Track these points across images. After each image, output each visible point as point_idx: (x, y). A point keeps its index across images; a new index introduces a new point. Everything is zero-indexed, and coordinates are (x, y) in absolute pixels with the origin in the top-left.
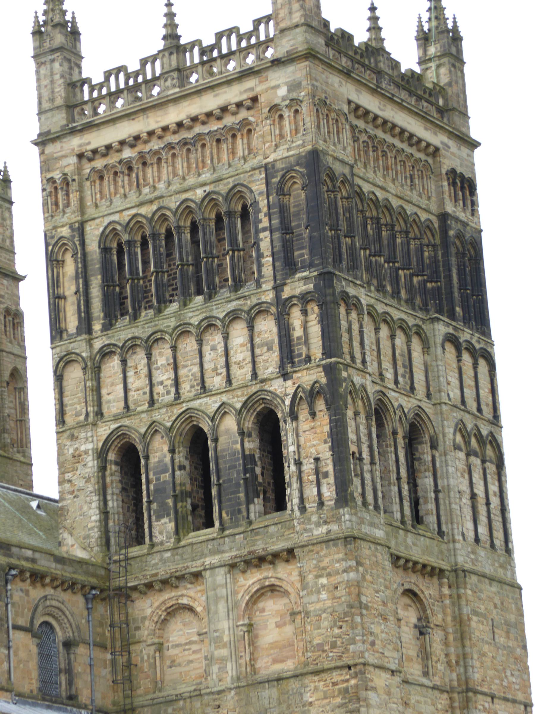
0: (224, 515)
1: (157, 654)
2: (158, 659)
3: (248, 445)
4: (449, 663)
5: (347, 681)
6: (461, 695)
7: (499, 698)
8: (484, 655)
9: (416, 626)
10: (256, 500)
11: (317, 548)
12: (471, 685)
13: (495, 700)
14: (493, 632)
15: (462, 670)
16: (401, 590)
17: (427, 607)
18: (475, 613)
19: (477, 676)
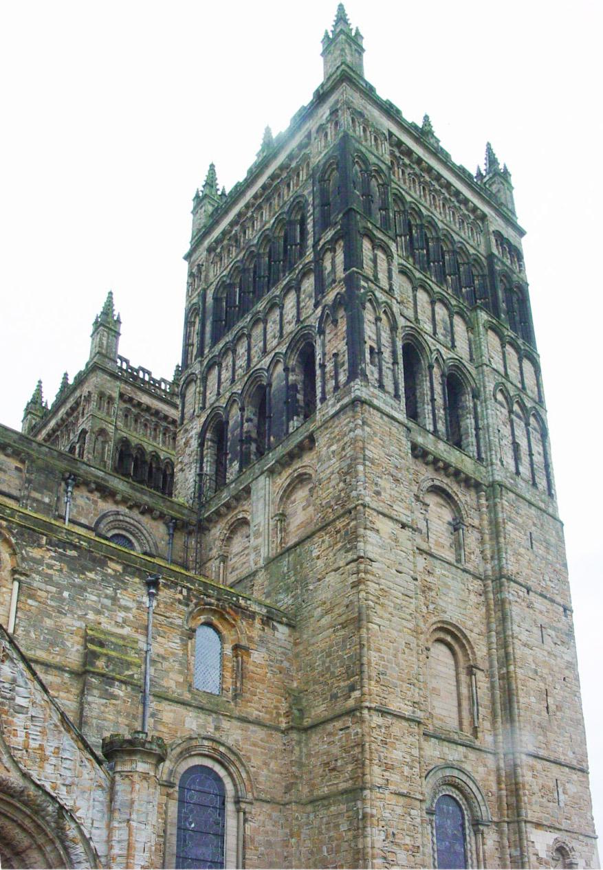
0: (272, 439)
1: (222, 564)
2: (222, 568)
3: (292, 378)
4: (484, 559)
5: (348, 524)
6: (494, 583)
7: (536, 593)
8: (519, 554)
9: (449, 523)
10: (295, 418)
11: (330, 424)
12: (505, 572)
13: (531, 593)
14: (532, 543)
15: (496, 562)
16: (429, 484)
17: (462, 508)
18: (510, 519)
19: (511, 567)
